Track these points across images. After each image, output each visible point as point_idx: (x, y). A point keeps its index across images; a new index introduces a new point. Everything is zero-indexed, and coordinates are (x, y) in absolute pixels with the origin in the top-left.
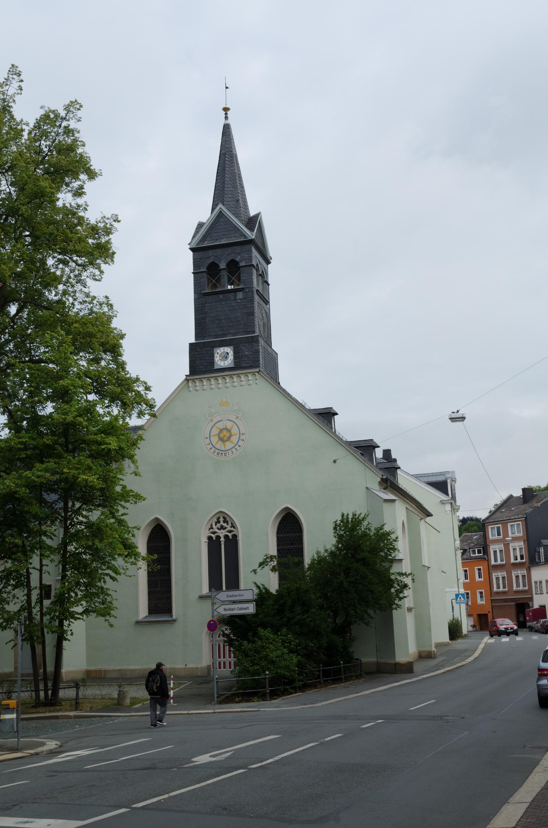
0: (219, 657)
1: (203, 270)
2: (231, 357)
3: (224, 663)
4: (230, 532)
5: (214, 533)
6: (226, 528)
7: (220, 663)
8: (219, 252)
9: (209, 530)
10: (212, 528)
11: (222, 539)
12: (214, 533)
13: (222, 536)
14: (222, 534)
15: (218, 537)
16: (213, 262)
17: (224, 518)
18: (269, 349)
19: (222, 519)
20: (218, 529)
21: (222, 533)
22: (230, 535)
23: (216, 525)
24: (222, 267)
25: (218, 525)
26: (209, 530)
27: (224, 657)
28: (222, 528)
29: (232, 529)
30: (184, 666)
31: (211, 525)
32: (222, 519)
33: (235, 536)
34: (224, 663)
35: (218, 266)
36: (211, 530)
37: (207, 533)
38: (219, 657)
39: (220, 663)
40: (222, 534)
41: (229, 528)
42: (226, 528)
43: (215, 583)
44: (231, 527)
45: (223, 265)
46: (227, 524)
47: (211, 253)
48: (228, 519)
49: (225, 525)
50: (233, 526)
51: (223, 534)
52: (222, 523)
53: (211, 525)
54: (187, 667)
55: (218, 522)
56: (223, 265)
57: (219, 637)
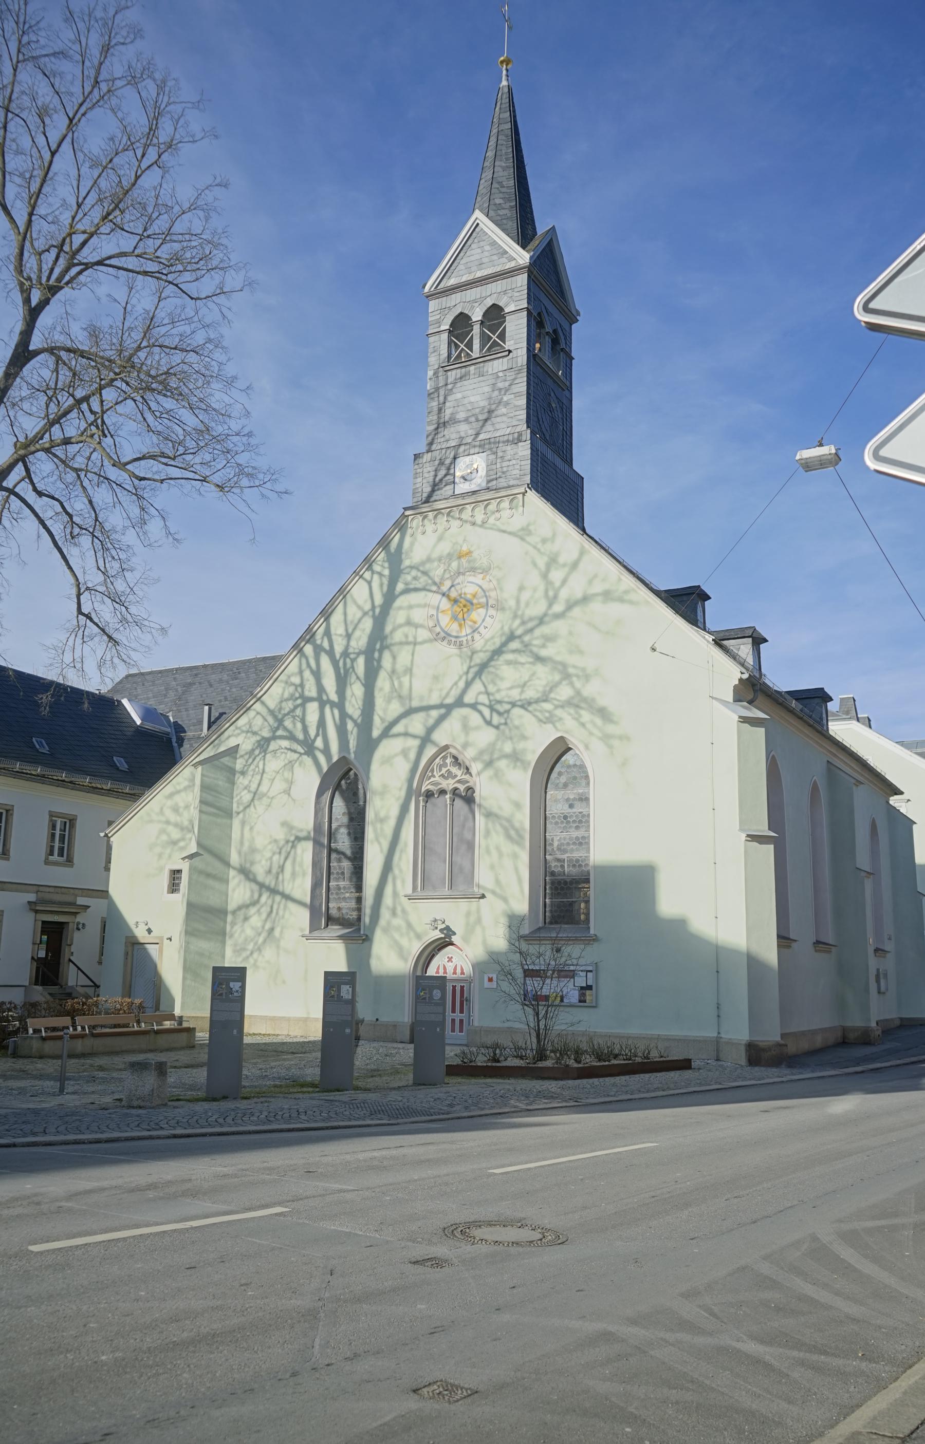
1: (443, 328)
2: (482, 472)
6: (456, 776)
8: (472, 294)
16: (461, 313)
18: (559, 462)
20: (442, 776)
24: (474, 320)
25: (444, 770)
28: (450, 775)
29: (467, 777)
35: (469, 318)
42: (456, 776)
46: (460, 769)
47: (456, 298)
49: (454, 770)
56: (477, 315)
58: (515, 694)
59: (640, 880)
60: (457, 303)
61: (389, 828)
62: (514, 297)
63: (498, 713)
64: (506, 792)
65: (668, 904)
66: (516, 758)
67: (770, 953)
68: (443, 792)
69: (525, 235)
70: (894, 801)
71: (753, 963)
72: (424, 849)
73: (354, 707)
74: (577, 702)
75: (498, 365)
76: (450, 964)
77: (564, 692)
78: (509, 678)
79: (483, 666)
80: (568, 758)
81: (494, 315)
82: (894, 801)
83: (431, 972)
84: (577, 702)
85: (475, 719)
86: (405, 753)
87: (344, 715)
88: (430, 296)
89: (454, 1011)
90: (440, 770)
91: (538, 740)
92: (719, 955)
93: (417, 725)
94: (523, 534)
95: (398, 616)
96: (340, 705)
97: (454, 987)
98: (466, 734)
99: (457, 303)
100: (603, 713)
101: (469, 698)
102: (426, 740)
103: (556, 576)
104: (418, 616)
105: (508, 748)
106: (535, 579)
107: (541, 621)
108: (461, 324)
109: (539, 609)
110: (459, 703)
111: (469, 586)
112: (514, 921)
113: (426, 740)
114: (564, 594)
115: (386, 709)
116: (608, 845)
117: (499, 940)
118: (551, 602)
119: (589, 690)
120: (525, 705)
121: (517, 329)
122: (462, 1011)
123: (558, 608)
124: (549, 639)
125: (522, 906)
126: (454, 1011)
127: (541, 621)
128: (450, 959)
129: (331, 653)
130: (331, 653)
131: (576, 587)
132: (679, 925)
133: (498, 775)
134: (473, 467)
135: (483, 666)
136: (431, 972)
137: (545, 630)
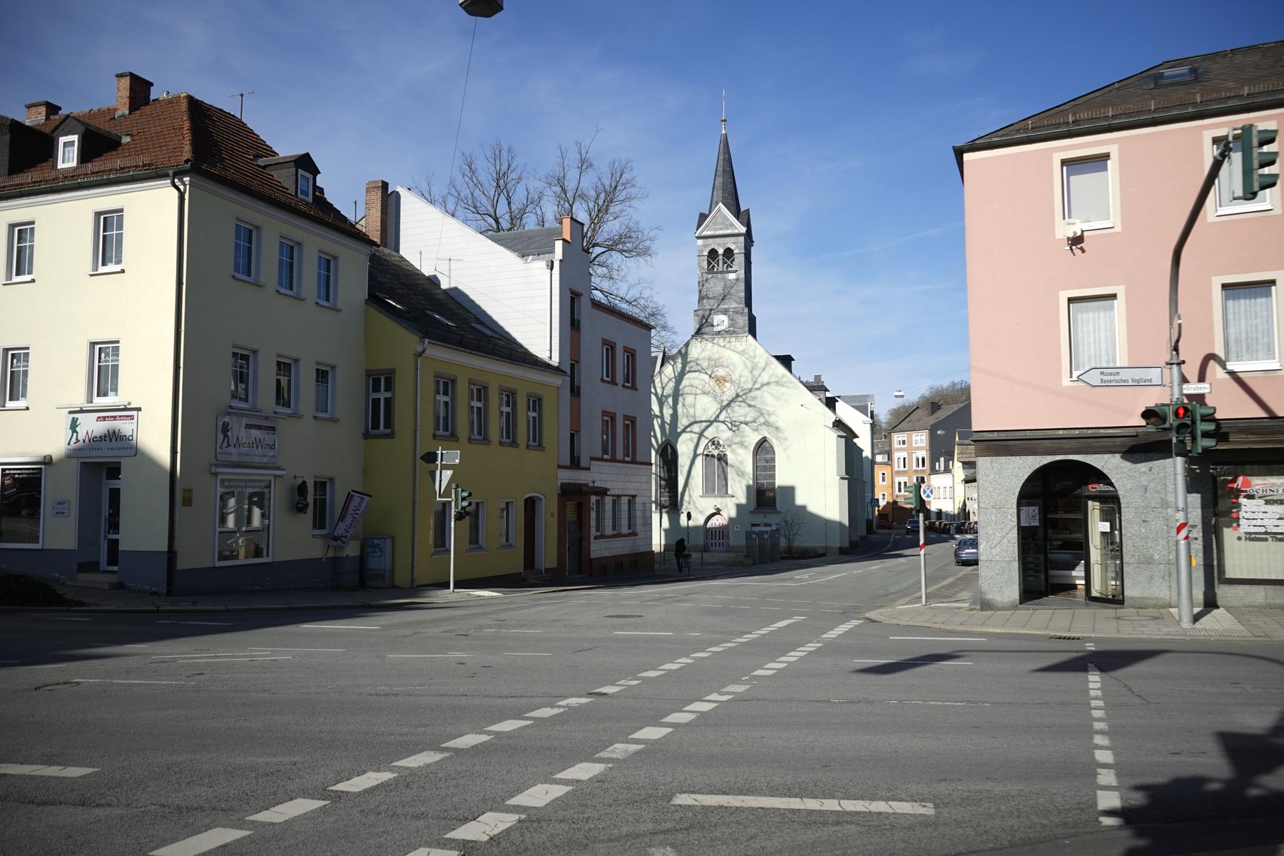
45: (721, 251)
56: (721, 251)
58: (742, 419)
59: (790, 491)
60: (713, 244)
61: (687, 468)
62: (737, 246)
63: (734, 426)
64: (742, 459)
65: (799, 501)
66: (742, 444)
67: (846, 522)
68: (713, 456)
69: (737, 213)
70: (855, 440)
71: (841, 524)
72: (707, 479)
73: (668, 419)
74: (767, 424)
75: (732, 276)
77: (762, 420)
78: (739, 412)
79: (729, 405)
80: (766, 444)
81: (729, 253)
82: (855, 440)
83: (709, 525)
84: (767, 424)
85: (723, 427)
86: (691, 439)
87: (663, 422)
88: (698, 238)
91: (754, 438)
92: (827, 523)
93: (696, 428)
94: (742, 353)
95: (685, 382)
96: (662, 417)
98: (723, 433)
99: (713, 244)
100: (777, 428)
101: (722, 418)
102: (701, 435)
103: (756, 373)
104: (696, 383)
105: (737, 440)
106: (746, 373)
107: (750, 390)
108: (713, 253)
109: (749, 386)
110: (716, 420)
111: (721, 372)
112: (739, 507)
113: (701, 435)
114: (760, 380)
115: (683, 421)
116: (781, 480)
117: (733, 513)
118: (755, 382)
119: (772, 419)
120: (746, 424)
121: (739, 260)
123: (757, 386)
124: (754, 398)
125: (743, 501)
127: (750, 390)
129: (656, 394)
130: (656, 394)
131: (765, 378)
132: (804, 508)
133: (733, 451)
134: (721, 321)
135: (729, 405)
136: (709, 525)
137: (752, 394)
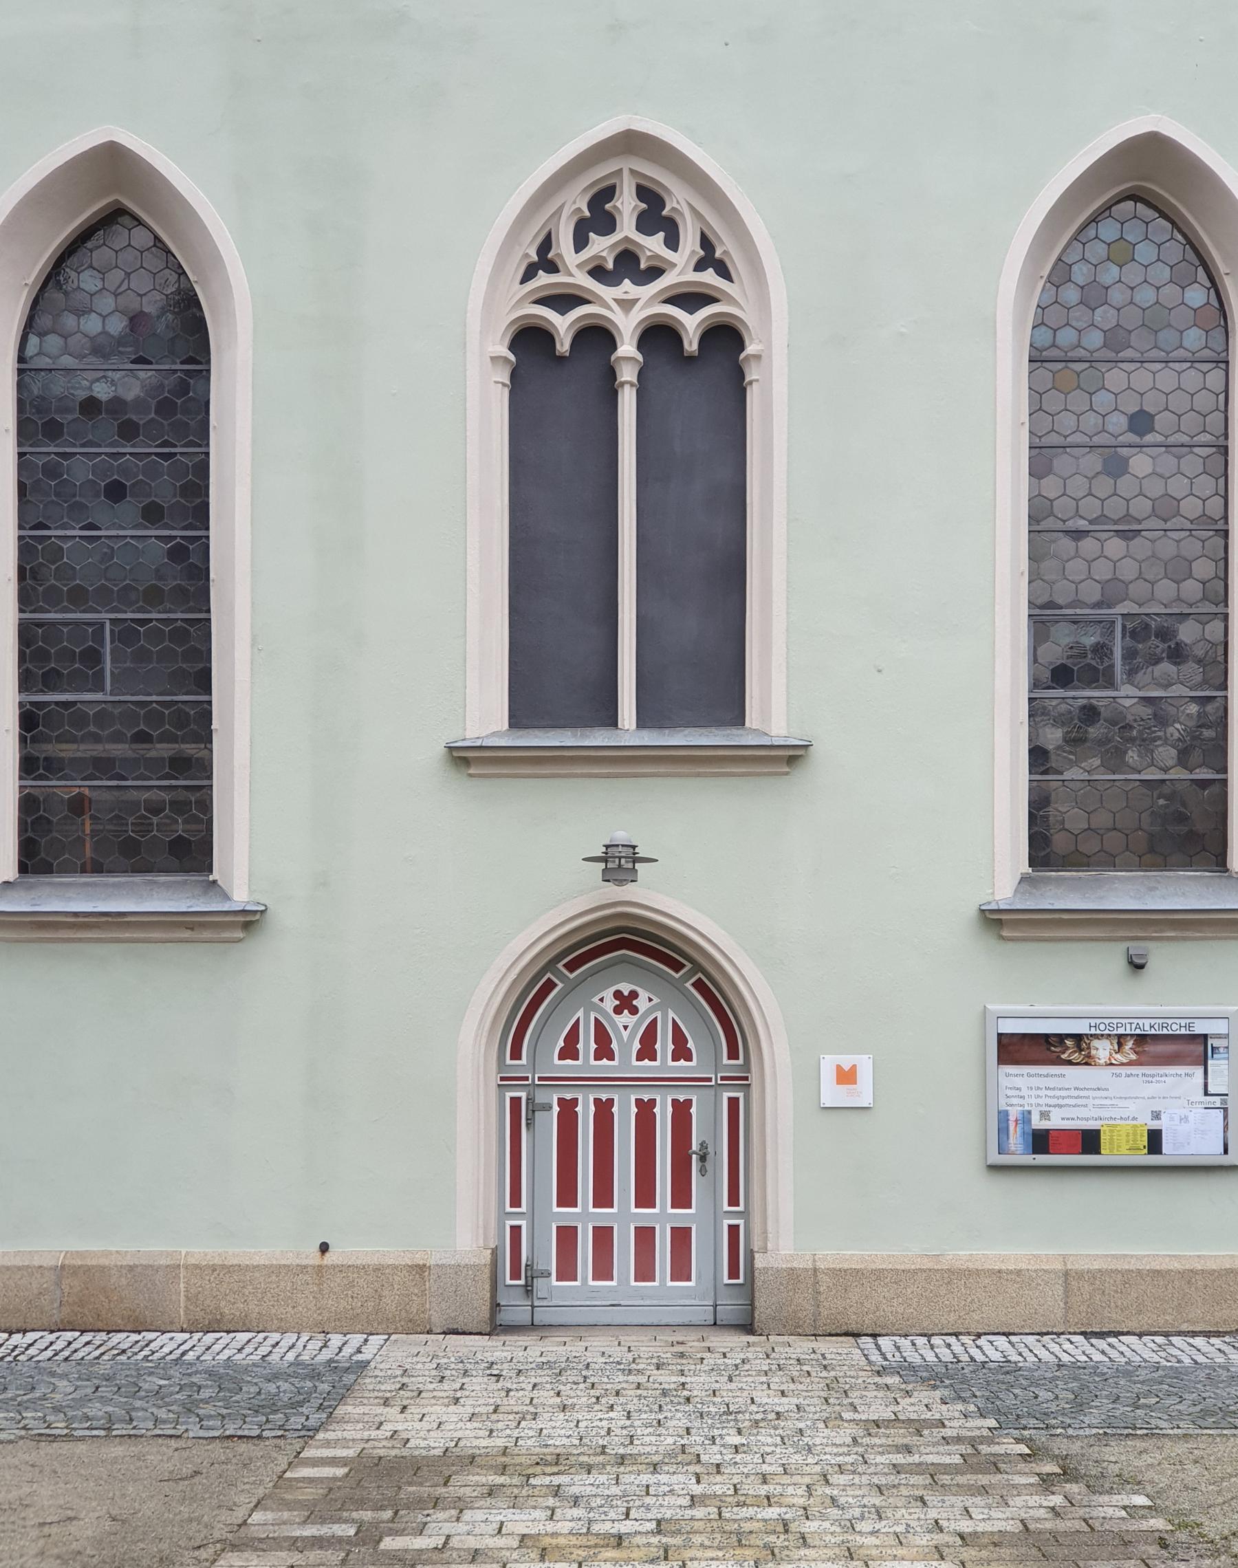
0: (567, 1196)
3: (603, 1236)
4: (691, 299)
5: (564, 301)
6: (655, 272)
7: (567, 1236)
9: (529, 274)
10: (552, 268)
11: (627, 348)
12: (564, 301)
13: (627, 328)
14: (627, 310)
15: (597, 337)
17: (644, 193)
19: (627, 206)
20: (598, 272)
21: (627, 305)
22: (691, 324)
23: (580, 242)
25: (601, 246)
26: (529, 274)
27: (603, 1196)
28: (628, 265)
29: (709, 277)
30: (314, 1258)
31: (546, 245)
32: (627, 206)
33: (726, 337)
34: (603, 1236)
36: (543, 279)
37: (516, 303)
38: (567, 1196)
39: (567, 1236)
40: (627, 310)
41: (681, 269)
43: (556, 679)
44: (700, 266)
46: (672, 242)
48: (679, 199)
49: (654, 244)
50: (709, 259)
51: (639, 315)
52: (627, 228)
53: (546, 245)
54: (330, 1258)
55: (598, 218)
57: (569, 1051)
76: (626, 1018)
89: (645, 1197)
90: (580, 242)
97: (646, 1111)
122: (681, 1197)
126: (645, 1197)
128: (626, 1003)
